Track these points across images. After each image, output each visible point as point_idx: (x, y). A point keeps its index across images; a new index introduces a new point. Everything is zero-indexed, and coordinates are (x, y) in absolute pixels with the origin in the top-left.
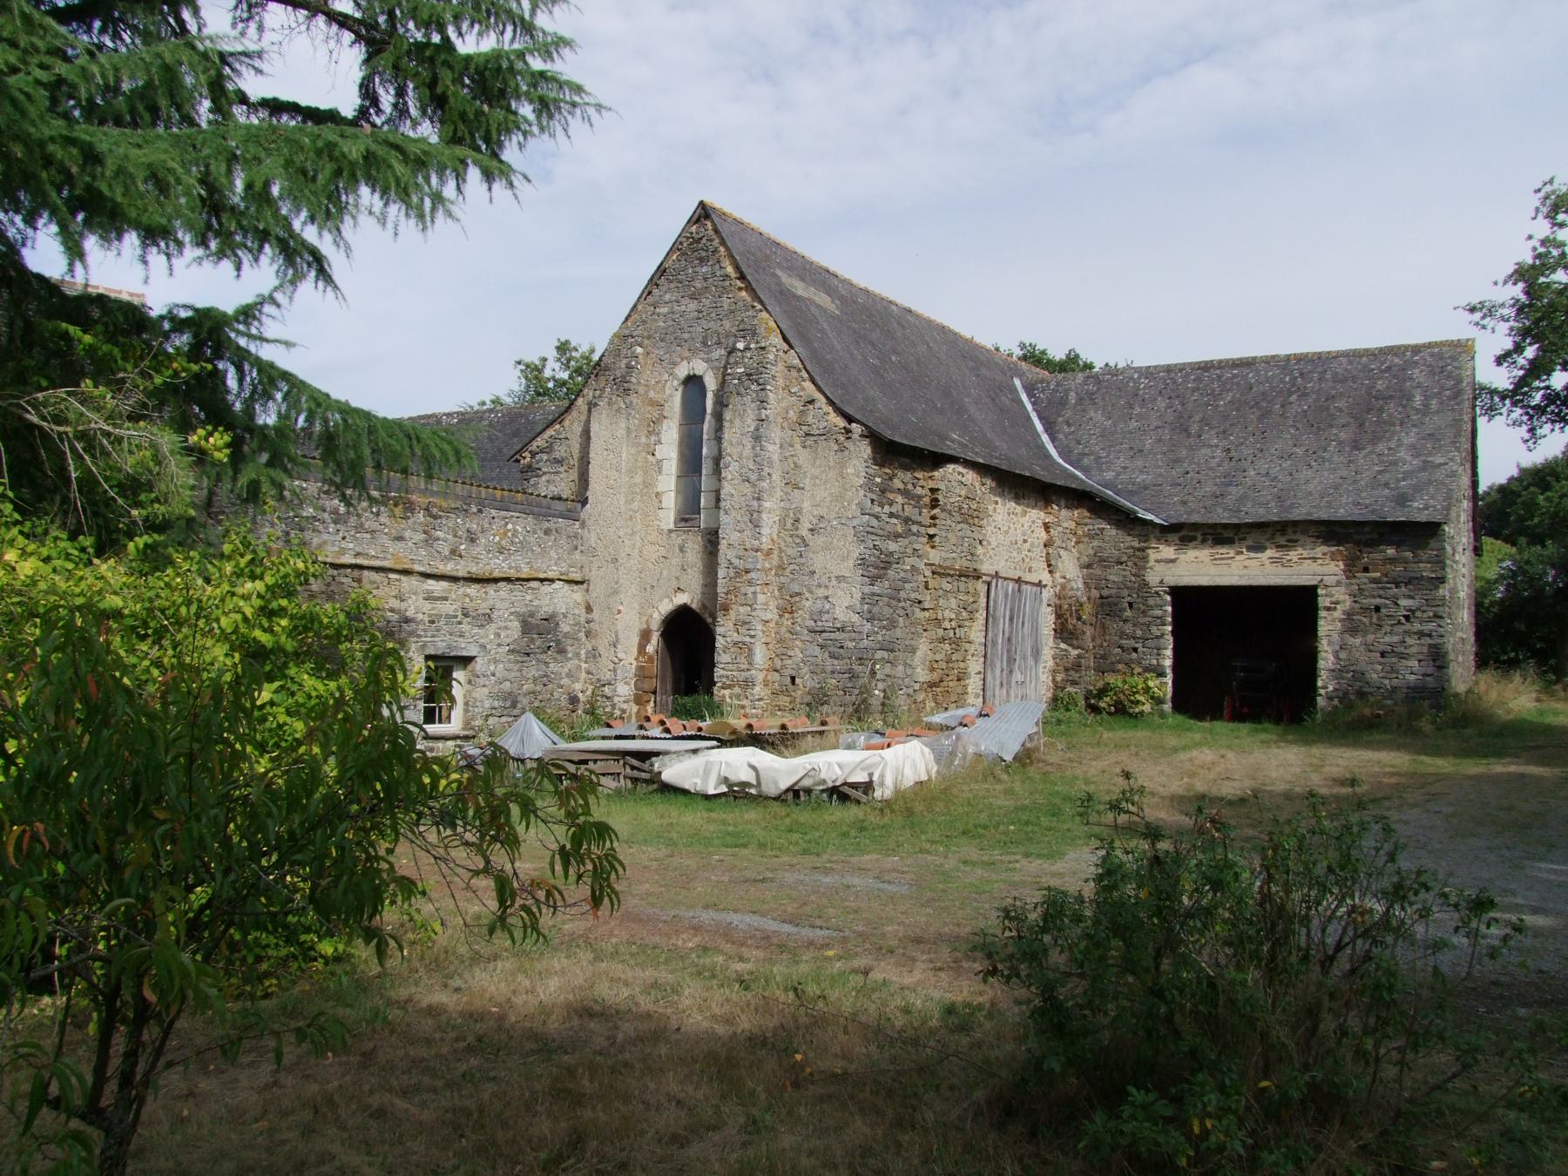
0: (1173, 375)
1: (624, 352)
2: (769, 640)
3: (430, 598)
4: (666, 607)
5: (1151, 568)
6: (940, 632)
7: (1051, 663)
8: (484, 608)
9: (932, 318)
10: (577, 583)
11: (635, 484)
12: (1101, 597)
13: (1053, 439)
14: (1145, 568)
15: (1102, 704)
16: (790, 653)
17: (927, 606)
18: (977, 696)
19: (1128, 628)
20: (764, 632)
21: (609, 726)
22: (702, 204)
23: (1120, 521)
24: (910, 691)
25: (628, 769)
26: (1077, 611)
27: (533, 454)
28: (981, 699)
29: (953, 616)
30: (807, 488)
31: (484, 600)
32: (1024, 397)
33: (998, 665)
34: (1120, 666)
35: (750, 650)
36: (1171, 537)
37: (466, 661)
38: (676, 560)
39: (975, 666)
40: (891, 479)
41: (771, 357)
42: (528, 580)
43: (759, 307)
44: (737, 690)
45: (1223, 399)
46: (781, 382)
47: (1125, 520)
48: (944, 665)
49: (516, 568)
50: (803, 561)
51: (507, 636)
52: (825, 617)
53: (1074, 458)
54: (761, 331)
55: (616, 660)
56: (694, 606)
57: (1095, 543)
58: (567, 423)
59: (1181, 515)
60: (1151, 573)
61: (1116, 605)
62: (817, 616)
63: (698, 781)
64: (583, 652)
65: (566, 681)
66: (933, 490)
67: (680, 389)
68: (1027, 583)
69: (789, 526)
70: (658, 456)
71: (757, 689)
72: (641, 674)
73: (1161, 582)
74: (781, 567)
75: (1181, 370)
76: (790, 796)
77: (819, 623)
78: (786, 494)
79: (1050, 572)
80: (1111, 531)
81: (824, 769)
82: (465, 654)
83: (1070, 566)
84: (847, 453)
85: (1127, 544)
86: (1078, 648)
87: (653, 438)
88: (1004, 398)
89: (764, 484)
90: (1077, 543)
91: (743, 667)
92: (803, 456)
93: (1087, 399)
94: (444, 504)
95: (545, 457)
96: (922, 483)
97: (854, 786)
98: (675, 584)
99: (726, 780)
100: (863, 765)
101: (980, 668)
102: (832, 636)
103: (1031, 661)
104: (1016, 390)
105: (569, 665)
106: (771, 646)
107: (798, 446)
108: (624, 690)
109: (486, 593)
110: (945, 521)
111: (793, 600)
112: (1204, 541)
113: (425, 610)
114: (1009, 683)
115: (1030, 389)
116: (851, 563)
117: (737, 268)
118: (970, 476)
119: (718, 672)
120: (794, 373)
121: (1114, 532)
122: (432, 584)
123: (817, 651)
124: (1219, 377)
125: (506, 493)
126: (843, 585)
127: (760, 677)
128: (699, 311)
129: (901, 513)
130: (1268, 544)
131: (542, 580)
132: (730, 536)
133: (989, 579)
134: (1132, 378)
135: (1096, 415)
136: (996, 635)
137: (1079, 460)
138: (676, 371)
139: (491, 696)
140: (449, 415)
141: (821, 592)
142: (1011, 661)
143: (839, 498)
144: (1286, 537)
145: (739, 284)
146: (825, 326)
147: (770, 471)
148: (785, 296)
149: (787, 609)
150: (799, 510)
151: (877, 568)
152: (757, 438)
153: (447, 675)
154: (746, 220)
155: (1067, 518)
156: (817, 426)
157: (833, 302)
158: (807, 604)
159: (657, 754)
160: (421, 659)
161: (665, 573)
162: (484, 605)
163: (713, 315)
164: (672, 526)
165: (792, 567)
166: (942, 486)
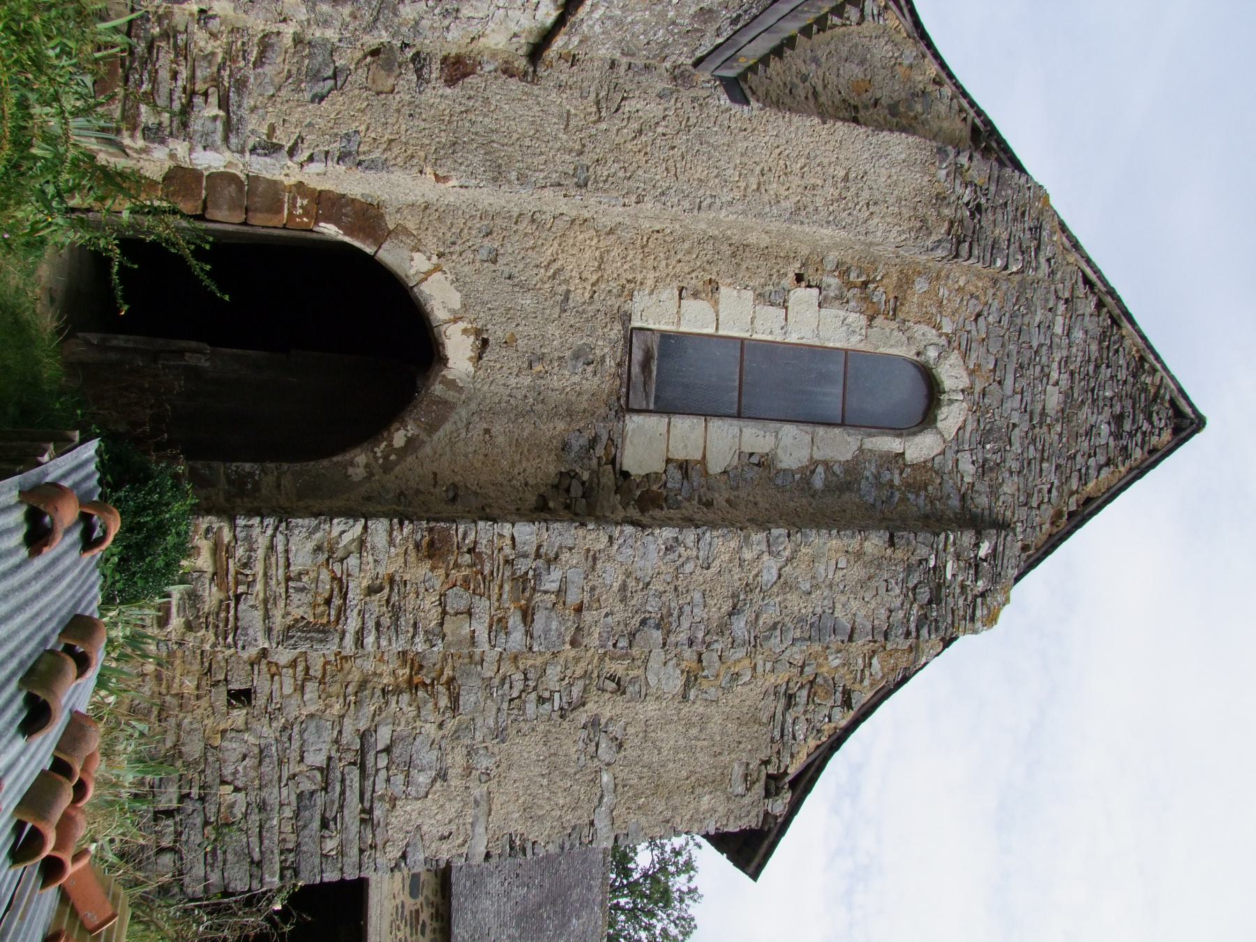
16: (311, 687)
22: (1198, 423)
77: (383, 761)
87: (833, 281)
91: (277, 614)
98: (496, 333)
102: (352, 798)
130: (421, 899)
144: (428, 922)
158: (430, 729)
161: (527, 301)
163: (1032, 452)
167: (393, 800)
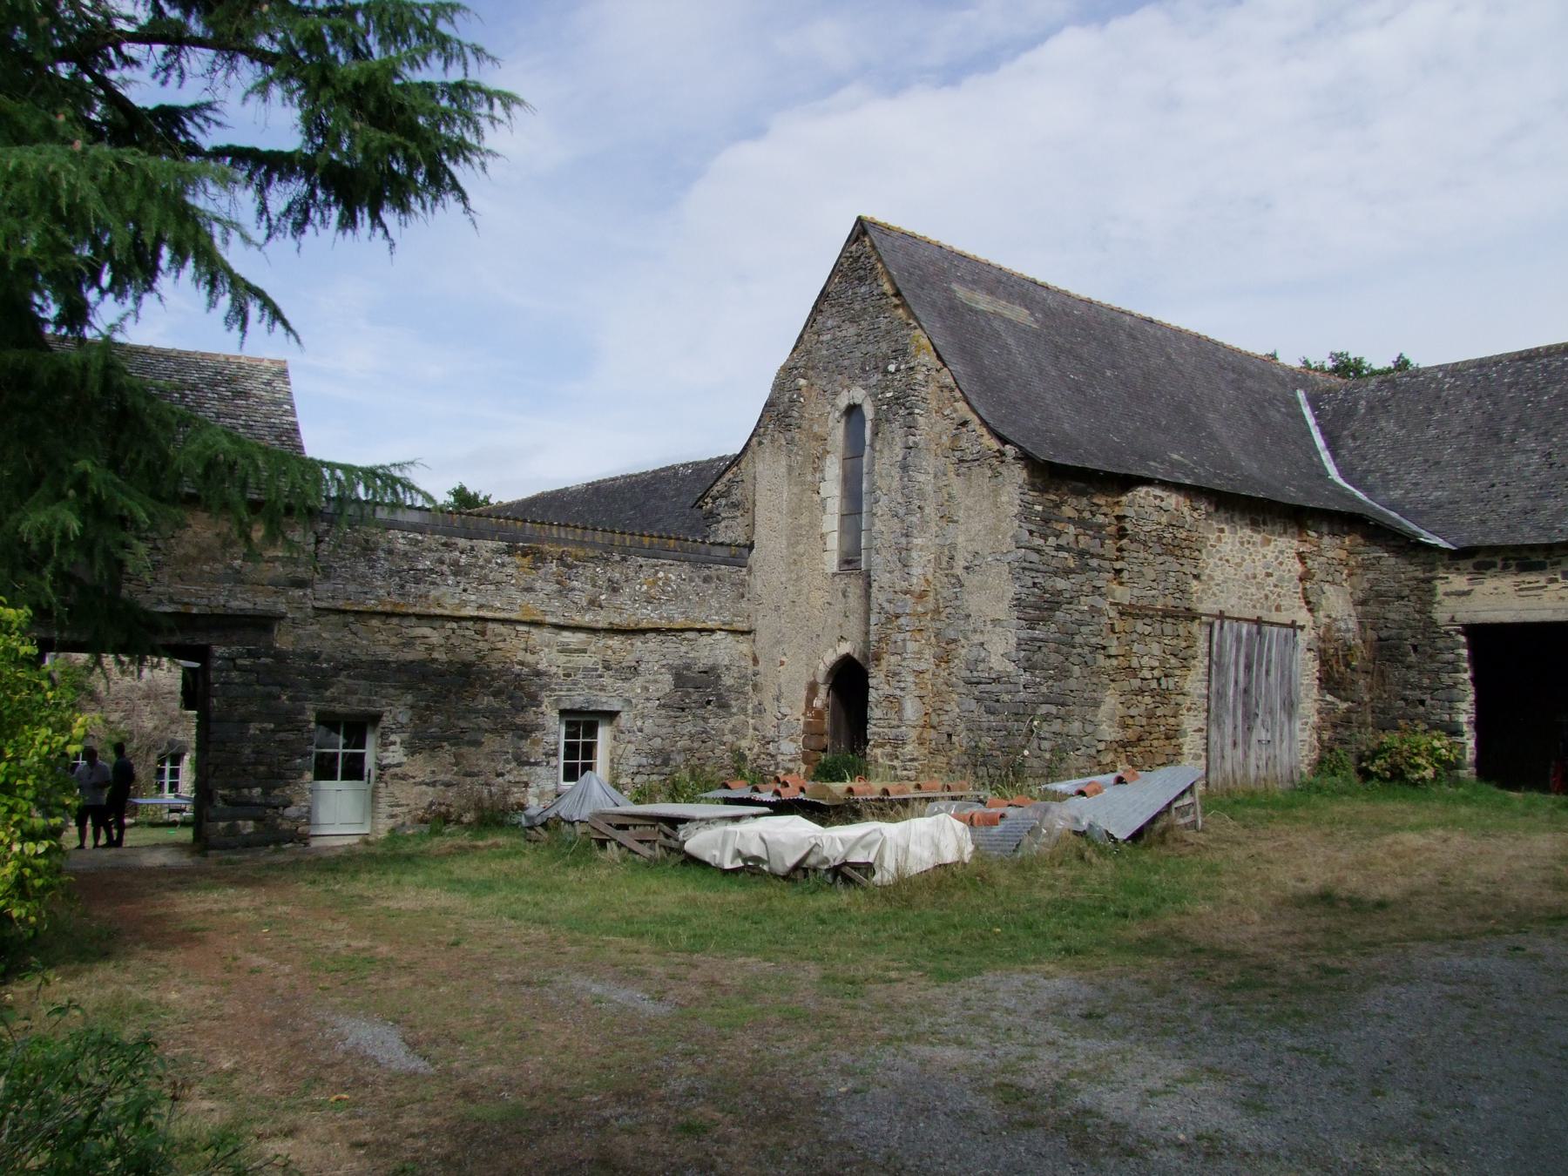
0: (1485, 370)
1: (788, 384)
2: (923, 693)
3: (565, 650)
4: (830, 658)
5: (1439, 603)
6: (1136, 683)
7: (1315, 719)
8: (630, 660)
9: (1184, 327)
10: (743, 633)
11: (800, 527)
12: (1380, 639)
13: (1335, 455)
14: (1431, 603)
15: (1373, 769)
17: (1113, 651)
18: (1197, 757)
19: (1413, 676)
20: (916, 684)
21: (727, 787)
22: (860, 220)
23: (1400, 547)
24: (1093, 751)
25: (662, 837)
26: (1345, 656)
27: (715, 499)
28: (1203, 762)
29: (1157, 664)
30: (962, 521)
31: (629, 652)
32: (1307, 411)
33: (1229, 721)
34: (1401, 722)
35: (901, 704)
36: (1462, 564)
37: (611, 716)
38: (839, 607)
39: (1191, 722)
40: (1057, 506)
41: (920, 377)
42: (682, 630)
43: (914, 324)
44: (888, 749)
45: (1547, 393)
46: (934, 404)
47: (1407, 546)
48: (1144, 721)
49: (668, 618)
50: (958, 603)
51: (657, 690)
52: (981, 666)
53: (1356, 476)
54: (912, 349)
55: (779, 715)
56: (856, 656)
57: (1371, 575)
58: (743, 465)
59: (1476, 537)
60: (1440, 609)
61: (1397, 648)
62: (972, 665)
63: (717, 853)
64: (750, 706)
65: (729, 738)
66: (1120, 518)
67: (843, 421)
68: (1272, 624)
69: (944, 564)
70: (823, 494)
71: (909, 748)
72: (811, 731)
73: (1453, 619)
74: (937, 611)
75: (1496, 364)
76: (800, 874)
77: (975, 674)
78: (941, 528)
79: (1310, 610)
80: (1389, 560)
81: (826, 843)
82: (606, 708)
83: (1338, 604)
84: (1000, 479)
85: (1409, 575)
86: (1346, 700)
87: (818, 475)
88: (1272, 413)
89: (914, 519)
90: (1350, 575)
91: (895, 723)
92: (957, 485)
93: (1379, 406)
94: (581, 553)
95: (724, 502)
96: (1105, 509)
97: (856, 866)
98: (838, 633)
99: (738, 854)
100: (863, 842)
101: (1201, 723)
102: (988, 688)
103: (1281, 716)
104: (1298, 403)
105: (733, 720)
106: (926, 700)
107: (952, 475)
108: (789, 748)
109: (632, 645)
110: (1135, 553)
111: (949, 647)
112: (1505, 567)
113: (559, 663)
114: (1247, 743)
115: (1314, 402)
116: (1005, 604)
117: (893, 284)
118: (1173, 500)
119: (871, 729)
120: (947, 394)
121: (1392, 561)
122: (567, 636)
123: (973, 705)
124: (1545, 367)
125: (655, 540)
126: (998, 629)
127: (913, 734)
128: (859, 335)
129: (1073, 545)
131: (700, 631)
132: (881, 578)
133: (1211, 619)
134: (1434, 379)
135: (1388, 425)
136: (1224, 686)
137: (1362, 479)
138: (837, 401)
139: (638, 752)
140: (685, 466)
141: (977, 638)
142: (1249, 717)
143: (993, 530)
145: (896, 301)
146: (1011, 341)
147: (922, 504)
148: (955, 312)
149: (944, 659)
150: (953, 546)
151: (1038, 609)
152: (905, 468)
153: (591, 730)
154: (919, 232)
155: (1332, 547)
156: (972, 451)
157: (1032, 314)
158: (963, 652)
159: (684, 820)
160: (555, 714)
162: (629, 657)
164: (835, 569)
165: (948, 610)
166: (1130, 512)
167: (991, 668)
